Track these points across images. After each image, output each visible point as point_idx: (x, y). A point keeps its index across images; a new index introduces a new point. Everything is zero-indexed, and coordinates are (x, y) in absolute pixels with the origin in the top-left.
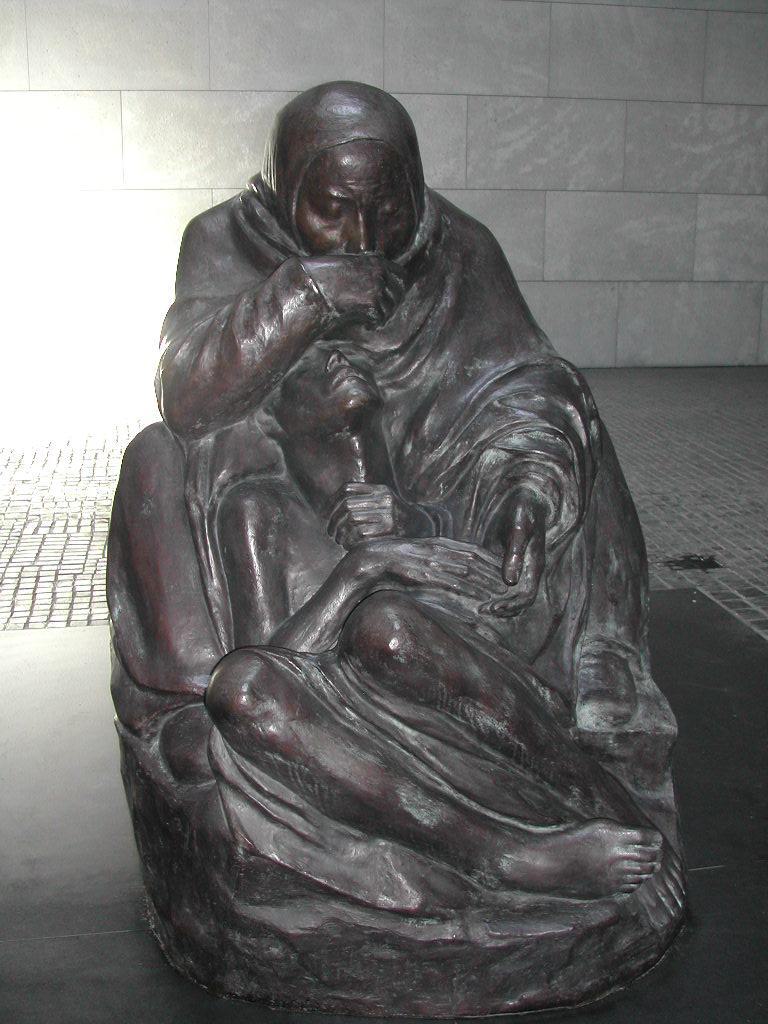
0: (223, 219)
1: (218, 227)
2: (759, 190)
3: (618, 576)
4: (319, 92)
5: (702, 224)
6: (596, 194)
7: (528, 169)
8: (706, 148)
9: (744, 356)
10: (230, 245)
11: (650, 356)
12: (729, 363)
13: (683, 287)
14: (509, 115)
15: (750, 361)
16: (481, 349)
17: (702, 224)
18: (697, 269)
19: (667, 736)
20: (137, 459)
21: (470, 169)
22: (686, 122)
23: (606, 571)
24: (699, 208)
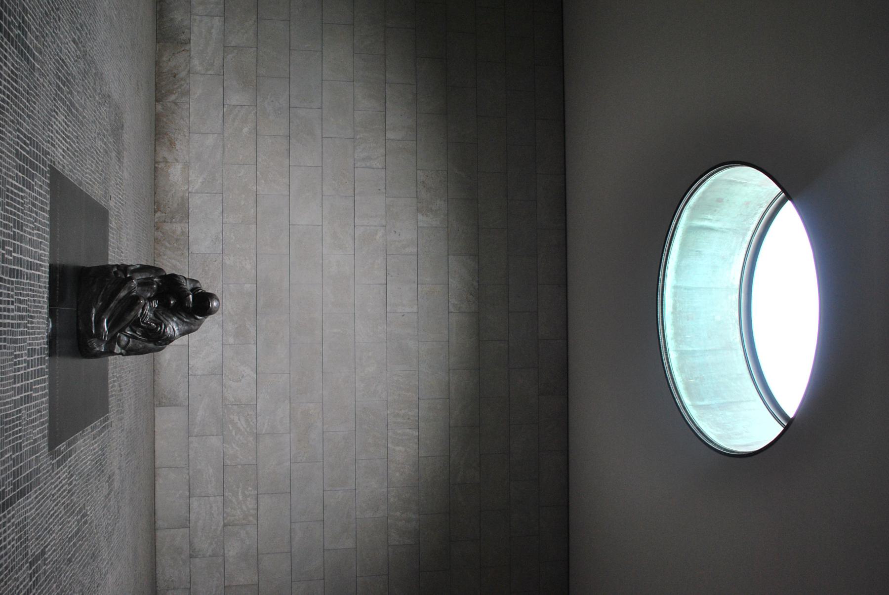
0: (200, 286)
1: (198, 285)
2: (226, 521)
3: (139, 346)
4: (218, 300)
5: (212, 499)
6: (222, 456)
7: (231, 428)
8: (241, 498)
9: (159, 523)
10: (195, 287)
11: (160, 482)
12: (156, 517)
13: (187, 493)
14: (250, 420)
15: (157, 526)
16: (177, 325)
17: (212, 499)
18: (194, 498)
19: (114, 350)
20: (161, 270)
21: (230, 406)
22: (250, 489)
23: (140, 344)
24: (218, 497)
